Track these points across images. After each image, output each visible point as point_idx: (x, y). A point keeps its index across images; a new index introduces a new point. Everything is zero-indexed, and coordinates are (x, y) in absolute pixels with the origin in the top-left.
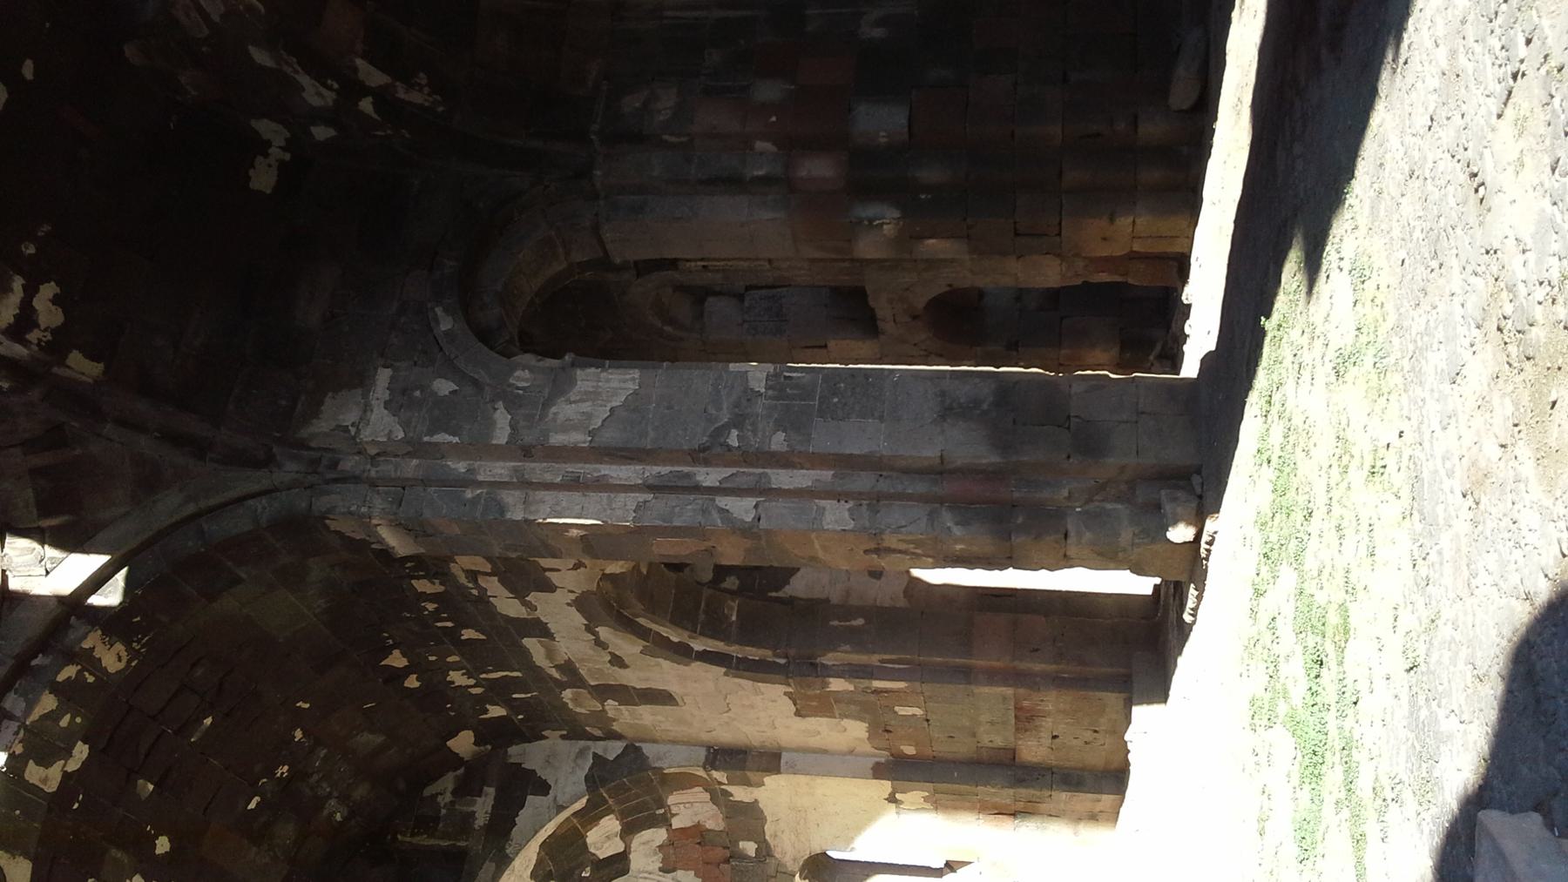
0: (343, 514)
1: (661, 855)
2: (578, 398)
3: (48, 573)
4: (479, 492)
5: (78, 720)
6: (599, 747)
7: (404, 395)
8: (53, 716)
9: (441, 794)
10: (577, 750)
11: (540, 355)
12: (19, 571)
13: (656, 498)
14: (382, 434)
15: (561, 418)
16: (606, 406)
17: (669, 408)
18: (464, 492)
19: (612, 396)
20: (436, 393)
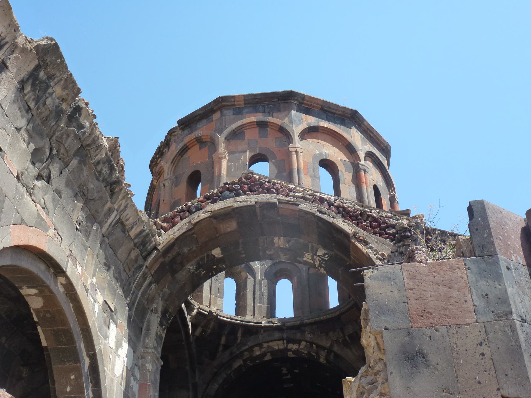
3: (335, 341)
8: (303, 353)
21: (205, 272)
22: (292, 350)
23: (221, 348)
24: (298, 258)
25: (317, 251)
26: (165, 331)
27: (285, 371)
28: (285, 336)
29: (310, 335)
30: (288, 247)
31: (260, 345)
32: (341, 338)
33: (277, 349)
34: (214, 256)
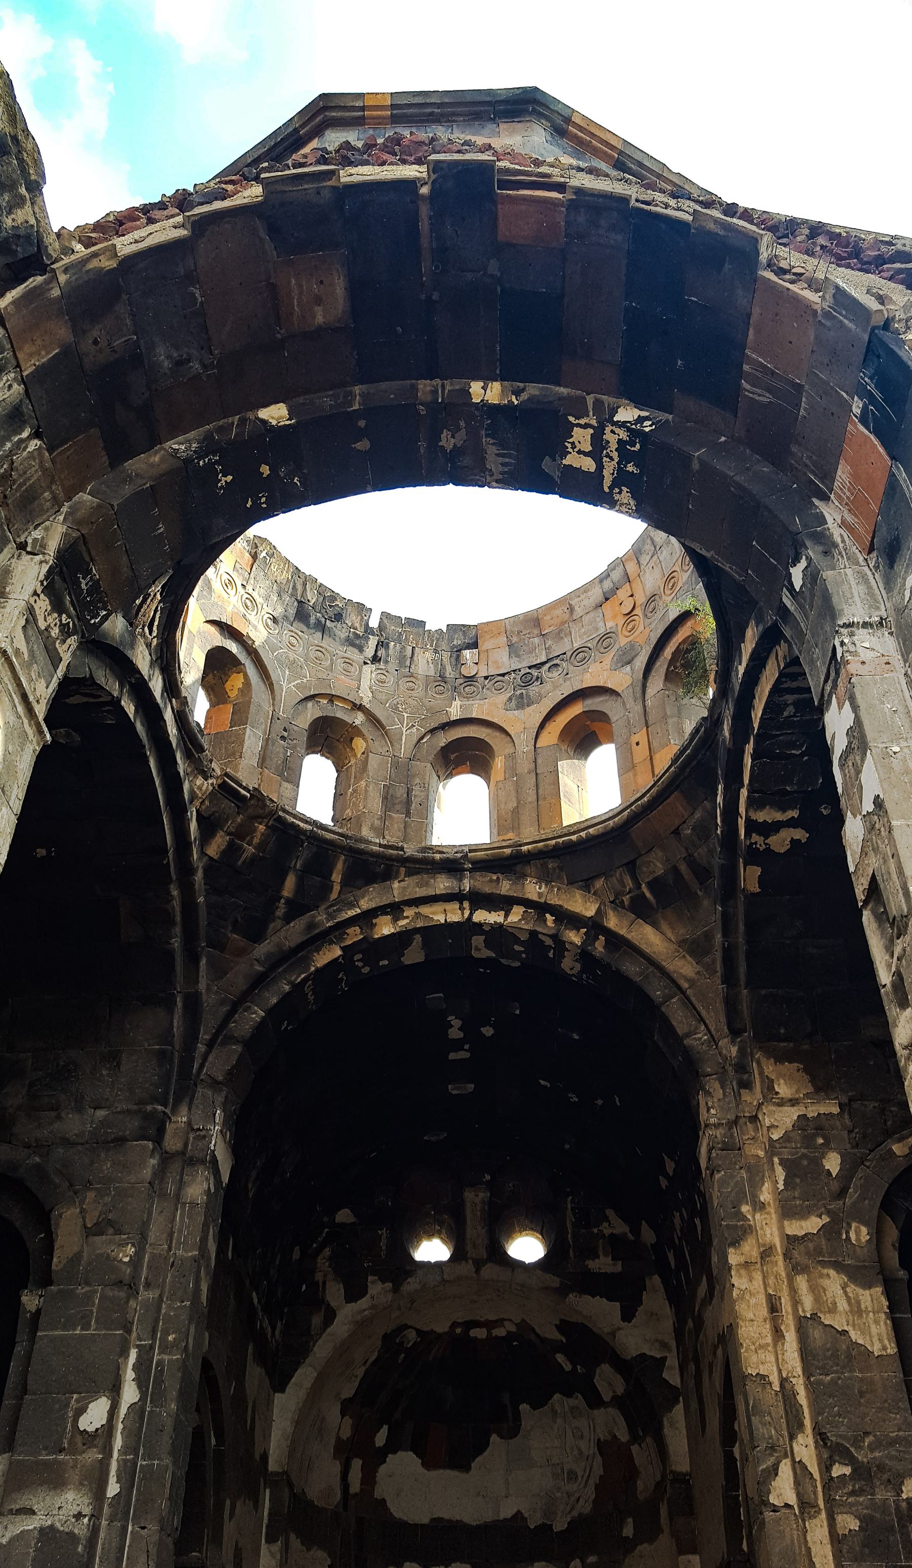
0: (707, 1104)
1: (609, 1438)
2: (851, 1295)
3: (612, 902)
4: (749, 1217)
5: (524, 956)
6: (673, 1361)
7: (816, 1129)
8: (518, 941)
9: (609, 1225)
10: (666, 1341)
11: (900, 1244)
12: (607, 884)
13: (776, 1394)
14: (772, 1120)
15: (825, 1282)
16: (848, 1325)
17: (861, 1394)
18: (747, 1204)
19: (860, 1329)
20: (824, 1158)
21: (229, 478)
22: (487, 928)
23: (281, 911)
24: (547, 464)
25: (614, 411)
26: (73, 641)
27: (455, 1033)
28: (466, 885)
29: (538, 887)
30: (516, 402)
31: (394, 909)
32: (628, 893)
33: (443, 921)
34: (264, 422)
